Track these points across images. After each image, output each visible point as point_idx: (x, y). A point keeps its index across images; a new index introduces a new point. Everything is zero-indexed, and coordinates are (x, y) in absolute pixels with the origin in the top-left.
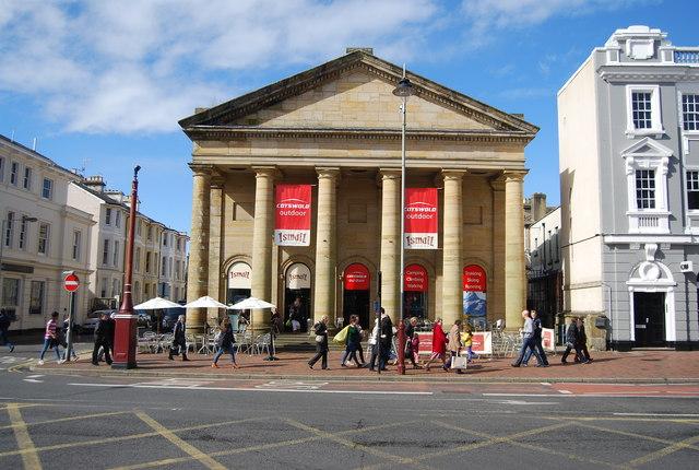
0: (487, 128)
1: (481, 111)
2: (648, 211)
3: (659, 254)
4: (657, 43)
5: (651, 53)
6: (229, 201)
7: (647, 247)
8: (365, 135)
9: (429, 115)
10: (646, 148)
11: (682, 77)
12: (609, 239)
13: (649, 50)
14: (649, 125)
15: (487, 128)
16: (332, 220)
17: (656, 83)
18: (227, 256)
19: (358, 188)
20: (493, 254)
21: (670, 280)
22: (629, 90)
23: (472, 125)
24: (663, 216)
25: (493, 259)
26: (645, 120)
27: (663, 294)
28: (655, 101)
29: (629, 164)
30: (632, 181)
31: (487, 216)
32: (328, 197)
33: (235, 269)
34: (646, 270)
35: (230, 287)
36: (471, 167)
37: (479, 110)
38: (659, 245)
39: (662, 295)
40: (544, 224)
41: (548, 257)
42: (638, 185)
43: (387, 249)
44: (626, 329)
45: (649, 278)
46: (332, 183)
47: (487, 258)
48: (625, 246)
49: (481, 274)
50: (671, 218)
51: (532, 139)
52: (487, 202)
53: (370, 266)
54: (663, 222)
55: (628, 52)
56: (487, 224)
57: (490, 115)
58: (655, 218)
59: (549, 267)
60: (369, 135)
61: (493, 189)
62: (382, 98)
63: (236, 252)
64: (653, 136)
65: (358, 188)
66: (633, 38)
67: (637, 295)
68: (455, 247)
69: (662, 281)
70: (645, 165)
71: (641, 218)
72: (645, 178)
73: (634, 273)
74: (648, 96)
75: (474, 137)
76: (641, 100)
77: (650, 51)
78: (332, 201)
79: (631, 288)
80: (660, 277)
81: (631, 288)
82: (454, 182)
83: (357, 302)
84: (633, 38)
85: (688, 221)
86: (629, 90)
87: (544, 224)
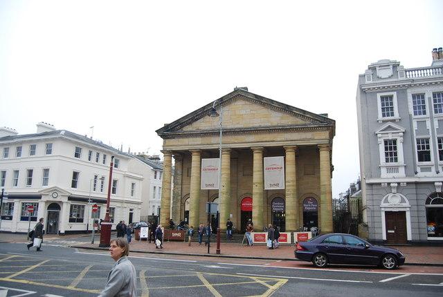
0: (308, 122)
1: (303, 114)
2: (394, 164)
9: (276, 119)
11: (410, 85)
13: (389, 72)
14: (392, 115)
17: (394, 91)
19: (241, 159)
21: (407, 204)
23: (299, 121)
30: (382, 147)
38: (399, 183)
39: (402, 215)
42: (386, 149)
43: (256, 190)
45: (394, 202)
54: (402, 171)
62: (253, 112)
64: (393, 121)
65: (241, 159)
69: (404, 205)
70: (390, 137)
72: (391, 146)
74: (391, 97)
75: (299, 128)
76: (387, 100)
79: (383, 209)
85: (418, 169)
86: (379, 95)
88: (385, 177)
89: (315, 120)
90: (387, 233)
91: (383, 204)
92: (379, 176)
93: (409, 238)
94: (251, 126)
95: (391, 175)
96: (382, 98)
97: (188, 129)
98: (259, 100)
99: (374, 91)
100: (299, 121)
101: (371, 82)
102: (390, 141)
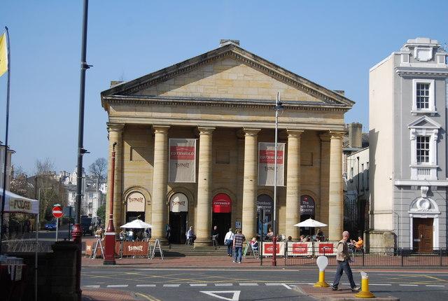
0: (319, 100)
1: (314, 89)
3: (429, 193)
4: (435, 50)
5: (430, 57)
6: (127, 147)
7: (422, 188)
8: (234, 105)
9: (280, 92)
10: (424, 122)
12: (399, 183)
13: (429, 54)
14: (427, 106)
15: (319, 100)
16: (209, 165)
18: (126, 187)
20: (320, 188)
21: (436, 209)
22: (414, 82)
23: (310, 98)
24: (433, 168)
25: (320, 192)
26: (425, 102)
27: (432, 219)
28: (431, 90)
29: (413, 133)
30: (414, 144)
31: (316, 160)
32: (207, 148)
33: (132, 196)
34: (421, 203)
35: (130, 209)
36: (307, 128)
37: (314, 89)
38: (430, 187)
39: (432, 220)
40: (358, 158)
41: (360, 183)
42: (418, 146)
44: (407, 242)
45: (422, 208)
46: (209, 138)
47: (316, 191)
48: (408, 187)
49: (312, 204)
50: (438, 169)
51: (349, 109)
52: (317, 150)
53: (232, 196)
54: (433, 172)
55: (415, 56)
56: (317, 166)
57: (322, 92)
58: (428, 169)
59: (361, 193)
60: (236, 105)
61: (321, 141)
63: (132, 185)
64: (429, 114)
66: (419, 46)
67: (414, 219)
68: (295, 185)
69: (433, 211)
70: (423, 133)
71: (419, 169)
72: (422, 141)
73: (413, 205)
74: (427, 86)
75: (310, 108)
77: (430, 56)
78: (209, 151)
79: (411, 215)
80: (430, 208)
81: (411, 215)
82: (296, 139)
83: (222, 220)
84: (419, 46)
86: (414, 82)
87: (358, 158)
88: (415, 178)
89: (330, 98)
90: (414, 242)
91: (413, 210)
92: (408, 177)
93: (436, 245)
94: (244, 97)
95: (422, 177)
96: (418, 85)
97: (151, 91)
98: (257, 63)
99: (411, 75)
100: (310, 98)
101: (407, 64)
102: (423, 138)
